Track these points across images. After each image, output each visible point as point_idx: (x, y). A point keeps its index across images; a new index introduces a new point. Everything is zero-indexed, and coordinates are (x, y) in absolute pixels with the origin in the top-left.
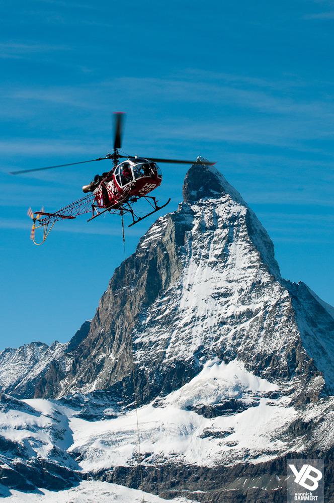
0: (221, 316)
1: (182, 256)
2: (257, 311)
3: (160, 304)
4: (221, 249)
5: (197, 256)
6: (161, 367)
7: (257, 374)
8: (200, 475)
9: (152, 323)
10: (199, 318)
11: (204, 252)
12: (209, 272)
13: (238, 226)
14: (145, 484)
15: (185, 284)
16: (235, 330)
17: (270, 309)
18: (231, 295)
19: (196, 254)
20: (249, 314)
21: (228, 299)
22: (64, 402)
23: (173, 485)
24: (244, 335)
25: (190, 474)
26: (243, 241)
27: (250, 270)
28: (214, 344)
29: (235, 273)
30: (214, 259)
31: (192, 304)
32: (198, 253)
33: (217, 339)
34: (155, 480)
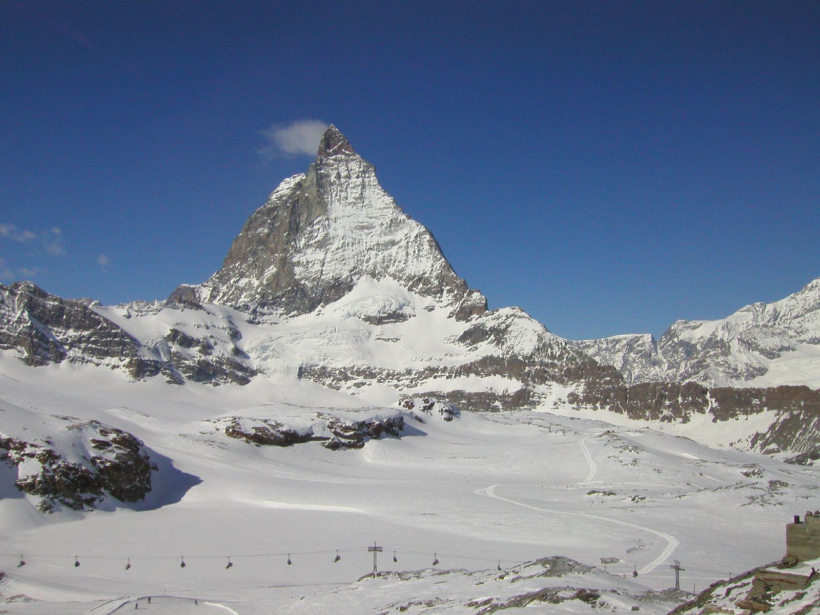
0: (368, 244)
3: (311, 232)
5: (338, 197)
6: (320, 282)
7: (410, 289)
9: (307, 246)
10: (348, 244)
11: (343, 194)
12: (349, 210)
15: (332, 216)
16: (383, 255)
17: (412, 240)
18: (374, 228)
19: (336, 196)
20: (393, 243)
21: (371, 231)
22: (146, 346)
23: (358, 385)
24: (392, 260)
28: (366, 265)
31: (341, 232)
33: (367, 262)
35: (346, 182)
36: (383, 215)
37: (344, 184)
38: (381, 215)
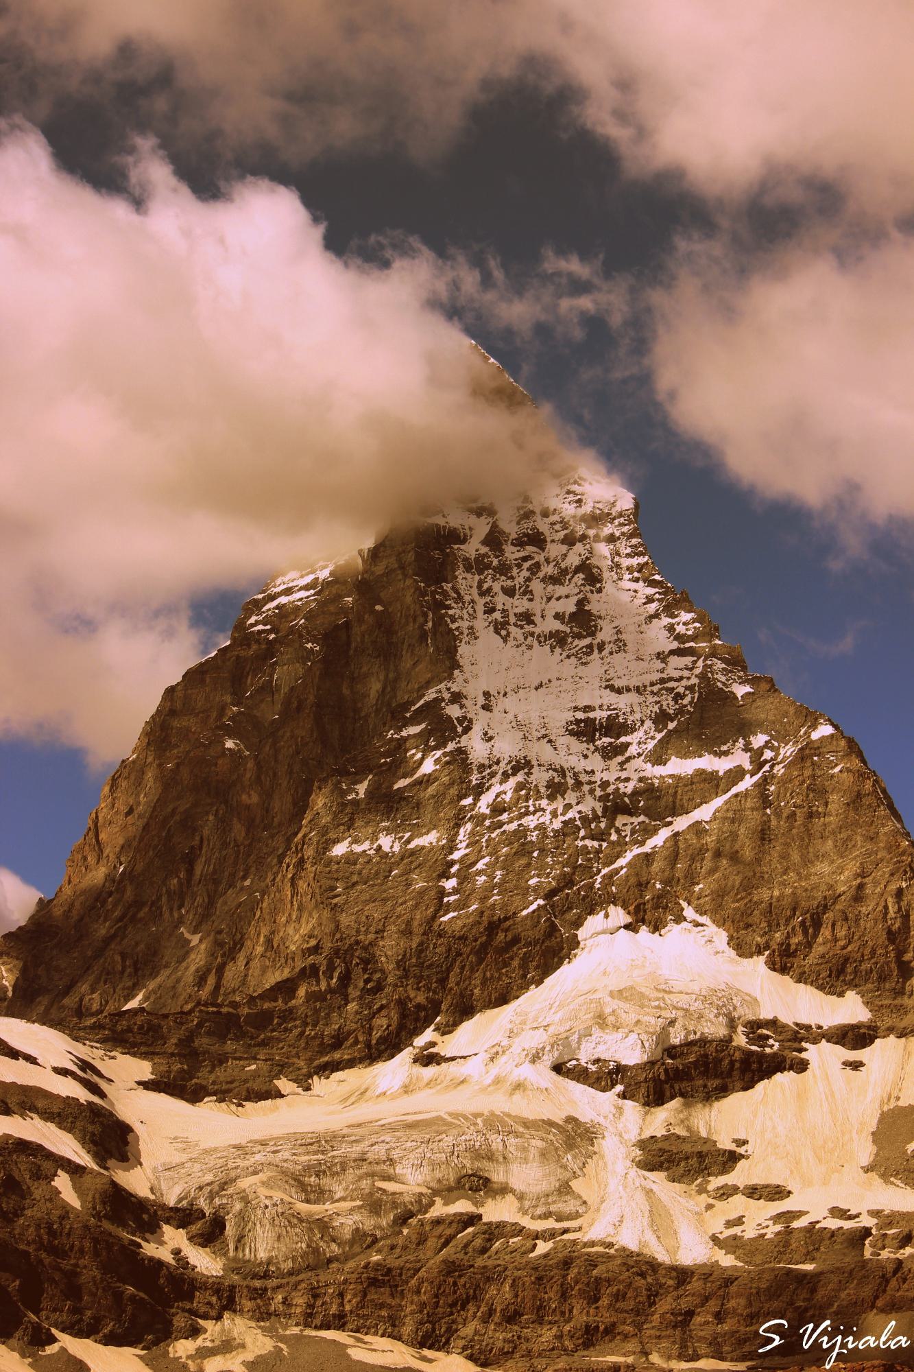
0: (610, 789)
1: (451, 612)
2: (737, 774)
4: (574, 599)
5: (497, 615)
8: (698, 1301)
12: (544, 661)
13: (611, 539)
14: (476, 1332)
15: (474, 691)
25: (653, 1296)
26: (637, 580)
27: (675, 661)
29: (626, 669)
30: (557, 626)
32: (500, 607)
34: (512, 1317)
35: (525, 559)
36: (671, 679)
37: (519, 566)
38: (662, 681)
